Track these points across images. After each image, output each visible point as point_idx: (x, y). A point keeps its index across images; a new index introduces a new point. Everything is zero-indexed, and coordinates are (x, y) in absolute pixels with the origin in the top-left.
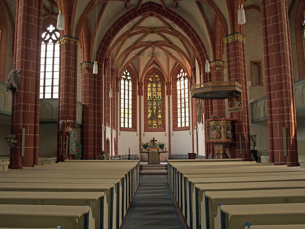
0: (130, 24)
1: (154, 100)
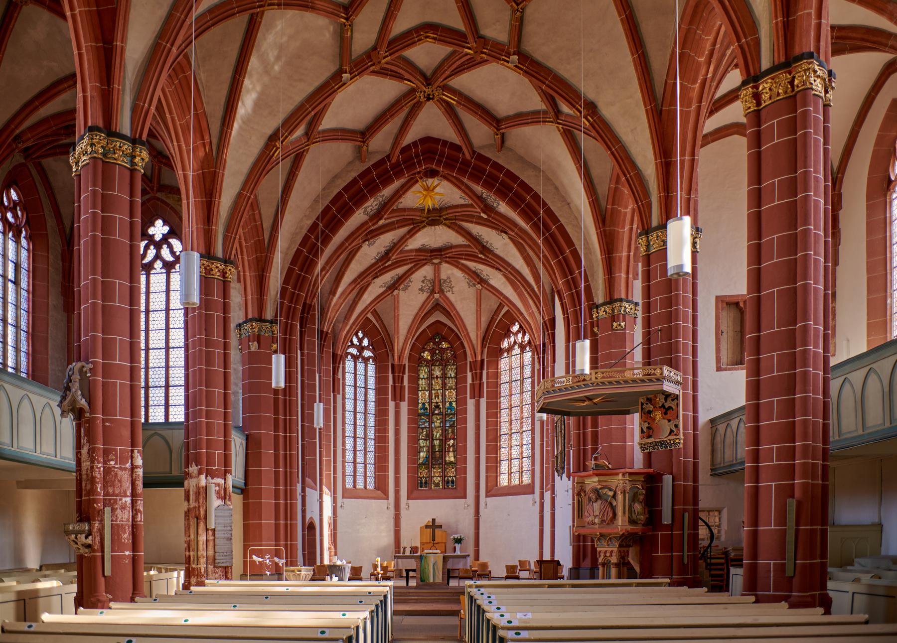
0: (372, 204)
1: (437, 412)
